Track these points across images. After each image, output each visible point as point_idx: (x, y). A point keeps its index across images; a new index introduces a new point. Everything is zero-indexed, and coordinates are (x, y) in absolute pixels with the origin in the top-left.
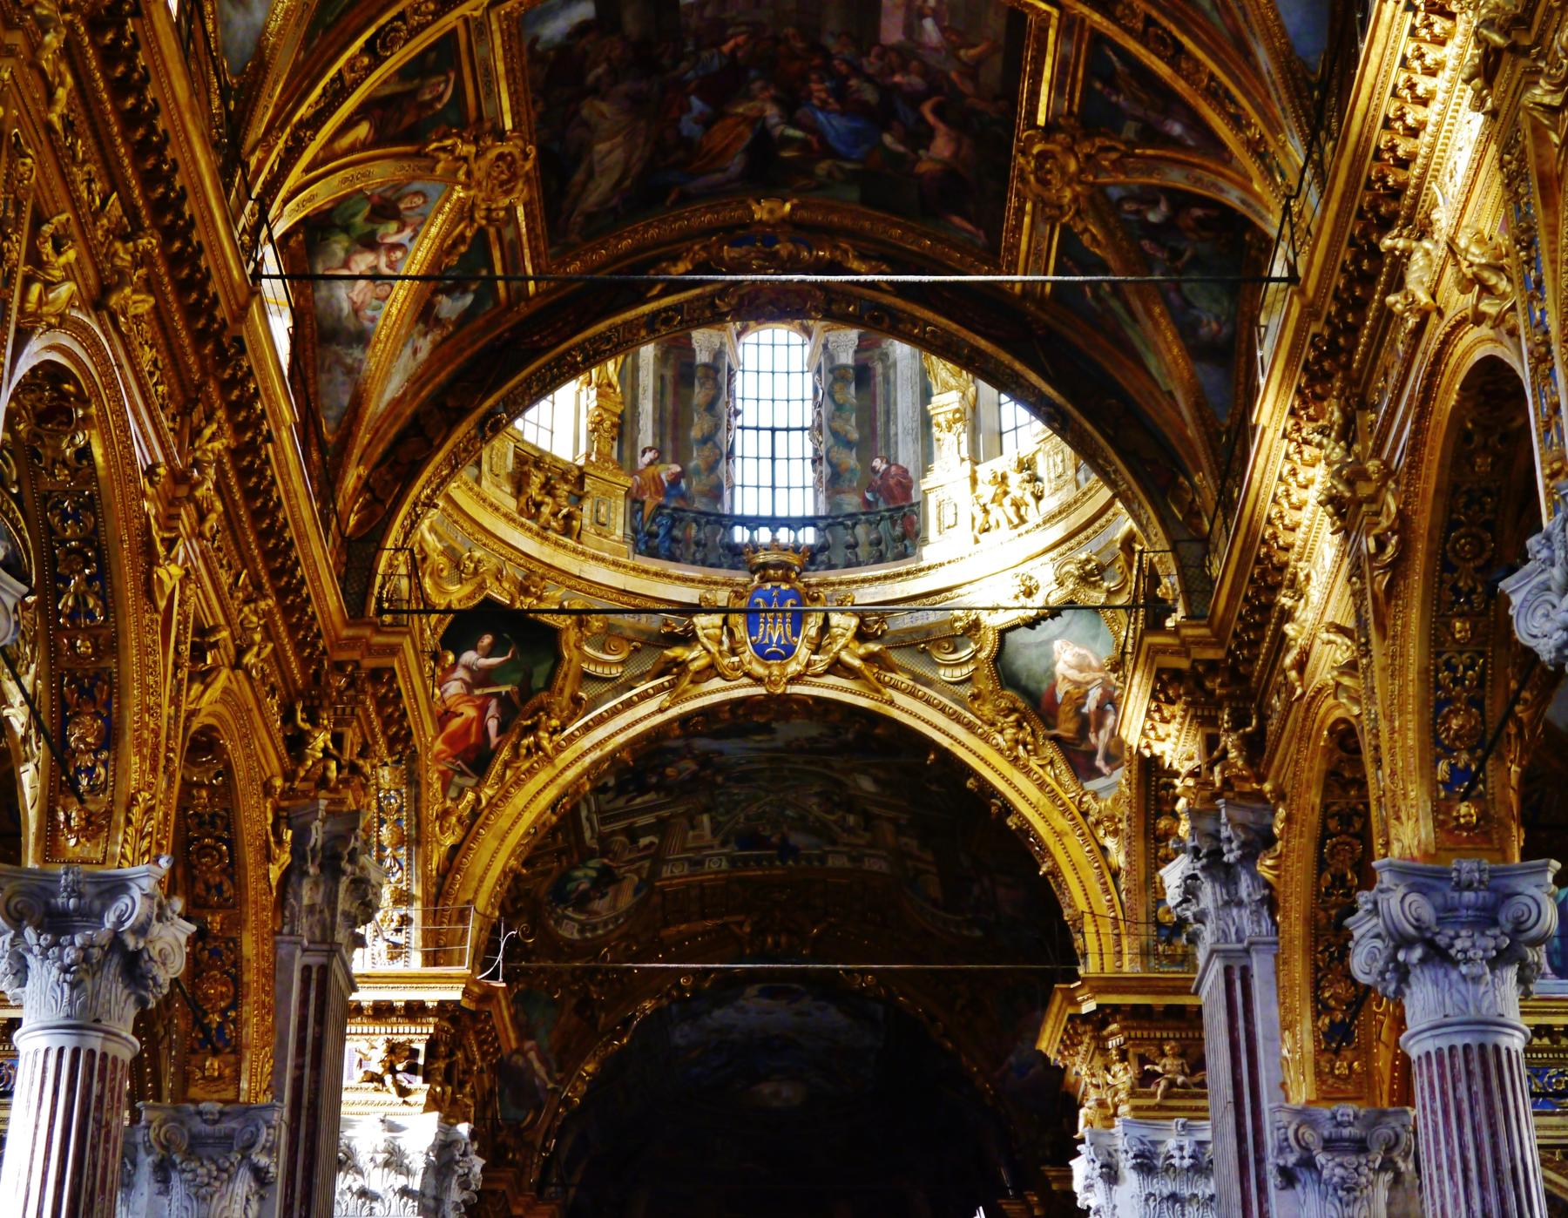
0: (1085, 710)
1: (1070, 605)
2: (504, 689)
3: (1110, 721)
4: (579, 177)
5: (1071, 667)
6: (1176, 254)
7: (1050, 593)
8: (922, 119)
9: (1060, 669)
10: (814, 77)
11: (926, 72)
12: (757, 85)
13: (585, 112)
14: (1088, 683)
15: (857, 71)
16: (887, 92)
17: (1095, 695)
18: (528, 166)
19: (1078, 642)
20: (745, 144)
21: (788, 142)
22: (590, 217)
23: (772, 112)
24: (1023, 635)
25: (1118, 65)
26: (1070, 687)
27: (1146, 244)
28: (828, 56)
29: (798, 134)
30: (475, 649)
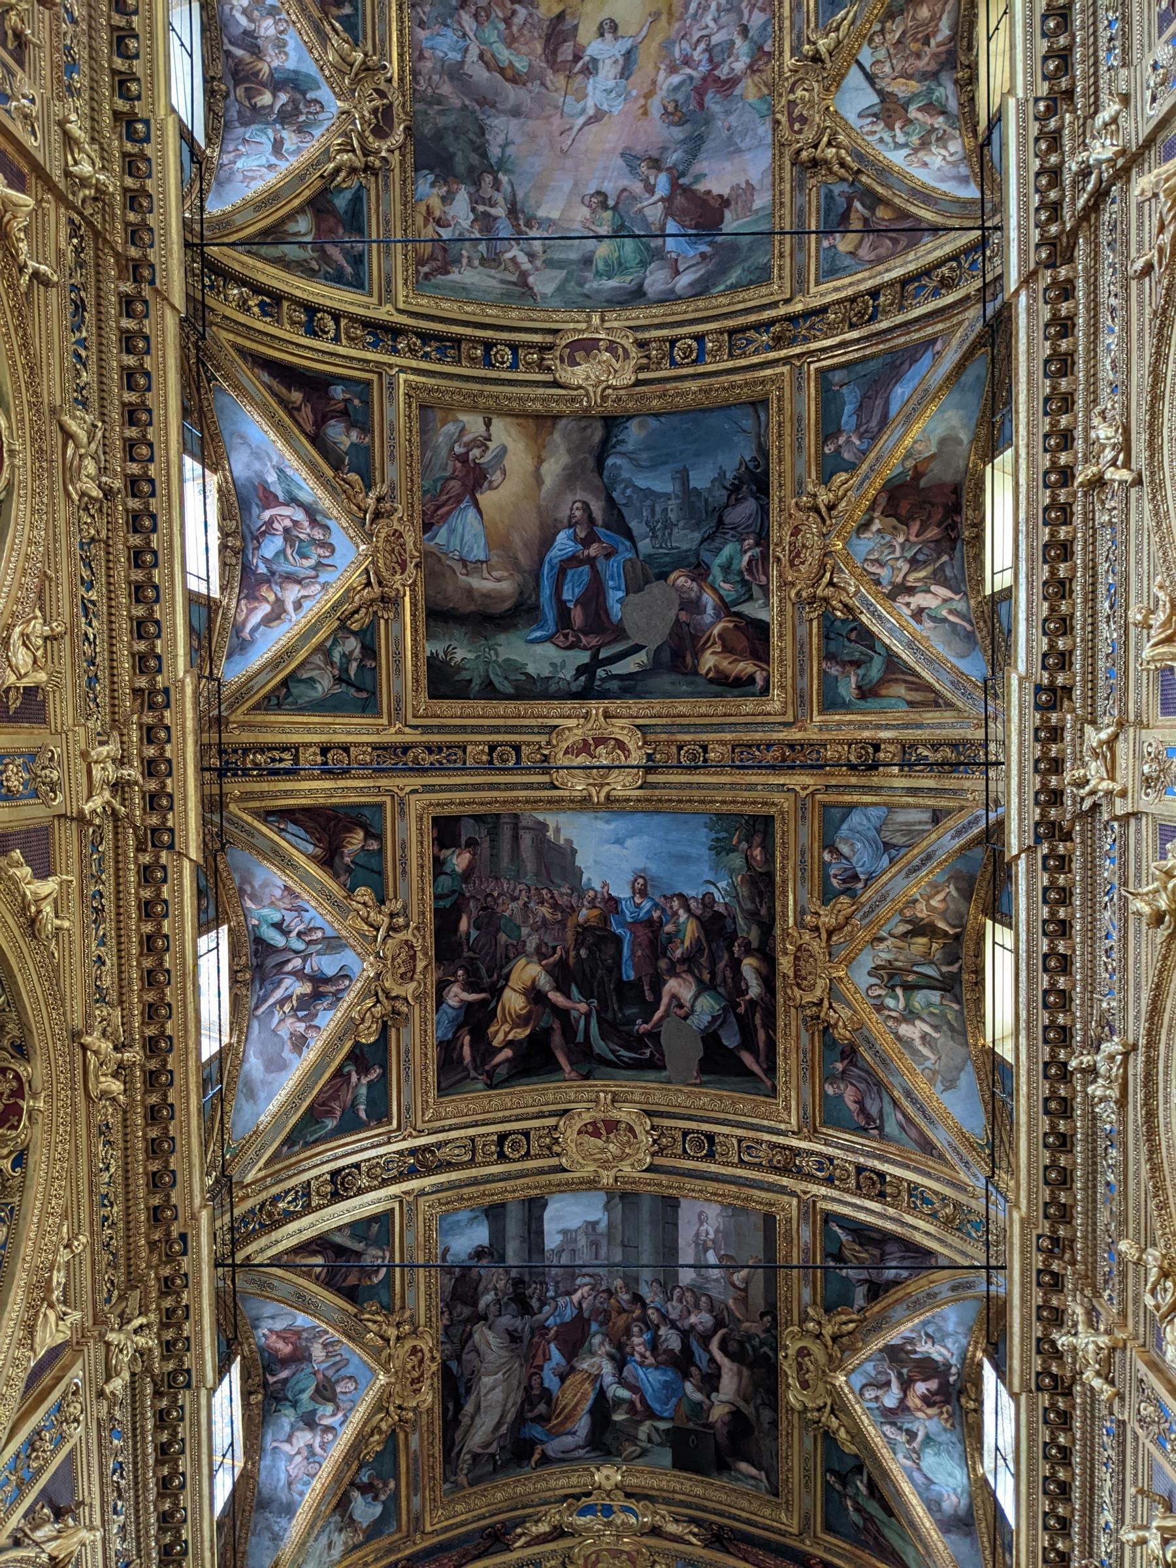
4: (469, 1408)
6: (911, 1435)
8: (712, 1360)
11: (711, 1311)
12: (597, 1340)
13: (476, 1336)
15: (664, 1317)
16: (685, 1334)
18: (434, 1367)
20: (587, 1405)
21: (618, 1402)
22: (476, 1457)
23: (608, 1368)
25: (844, 1237)
27: (887, 1429)
28: (644, 1306)
29: (624, 1393)
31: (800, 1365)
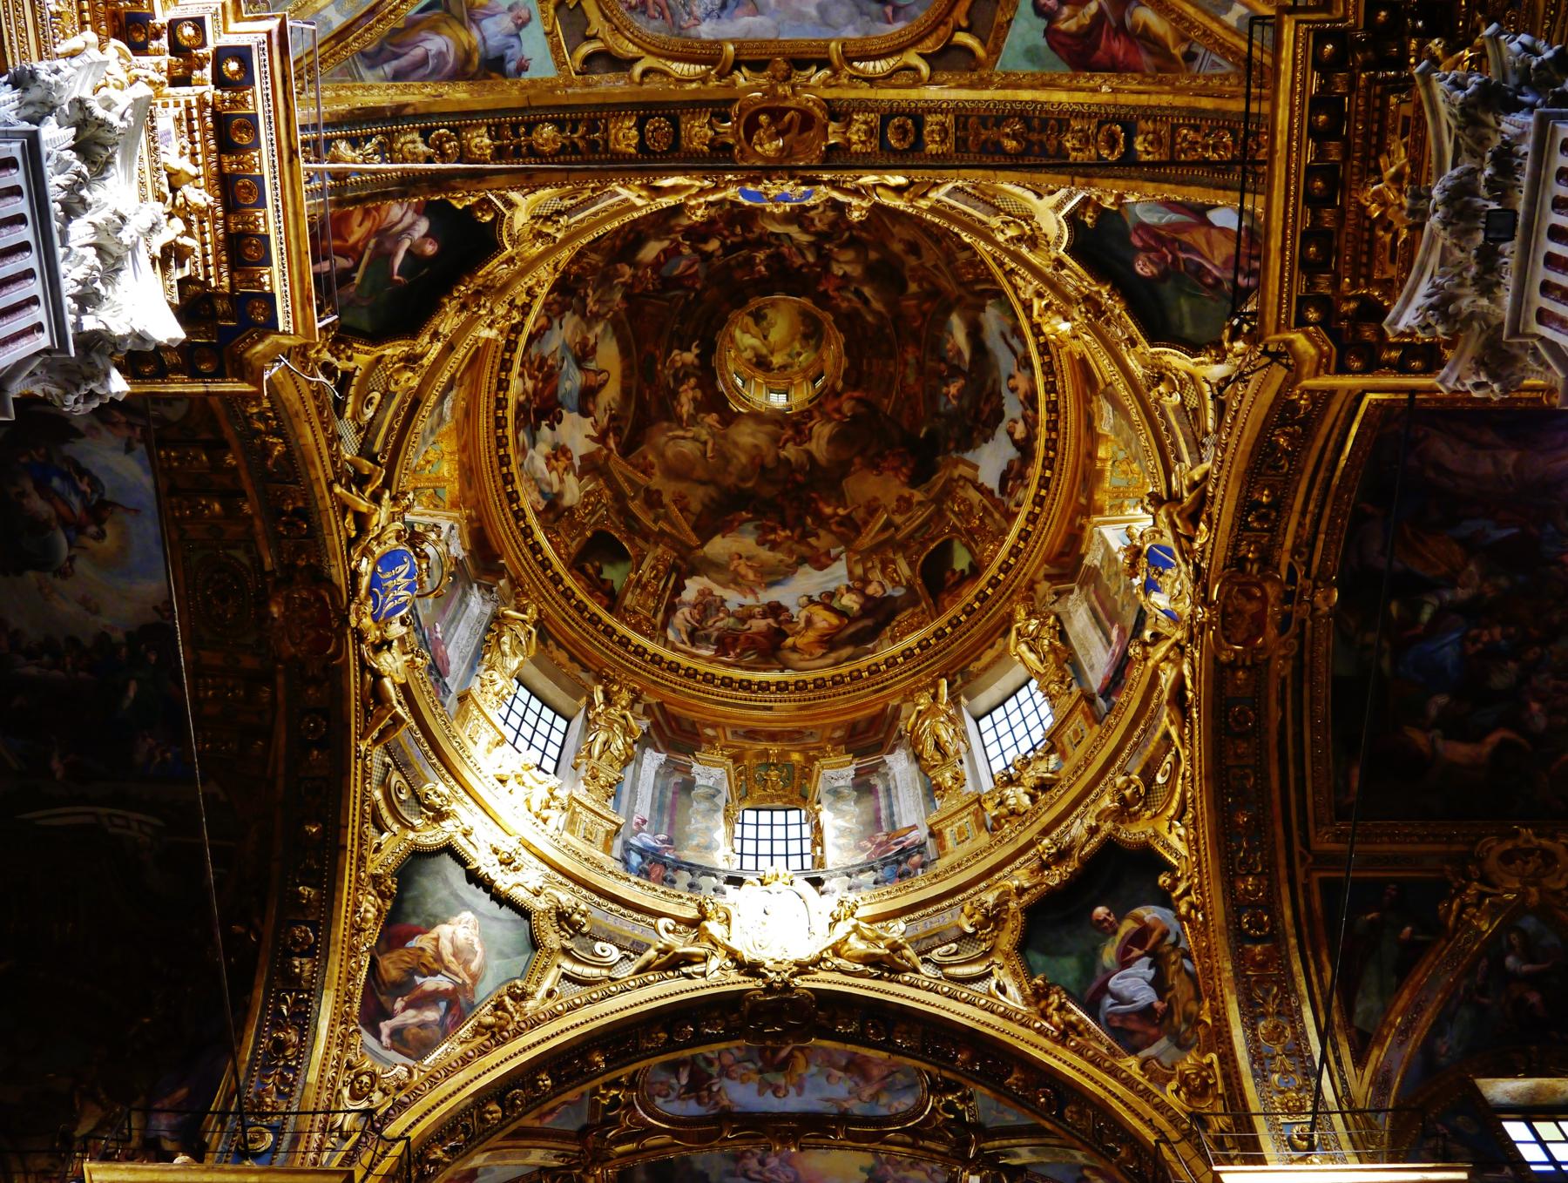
0: (419, 980)
1: (523, 912)
2: (358, 276)
3: (431, 1015)
5: (452, 942)
7: (524, 882)
9: (443, 931)
10: (1512, 630)
12: (1503, 582)
14: (447, 969)
17: (440, 983)
19: (484, 939)
21: (1417, 610)
24: (455, 873)
26: (430, 951)
27: (1484, 963)
29: (1426, 614)
30: (426, 236)
31: (1531, 852)
